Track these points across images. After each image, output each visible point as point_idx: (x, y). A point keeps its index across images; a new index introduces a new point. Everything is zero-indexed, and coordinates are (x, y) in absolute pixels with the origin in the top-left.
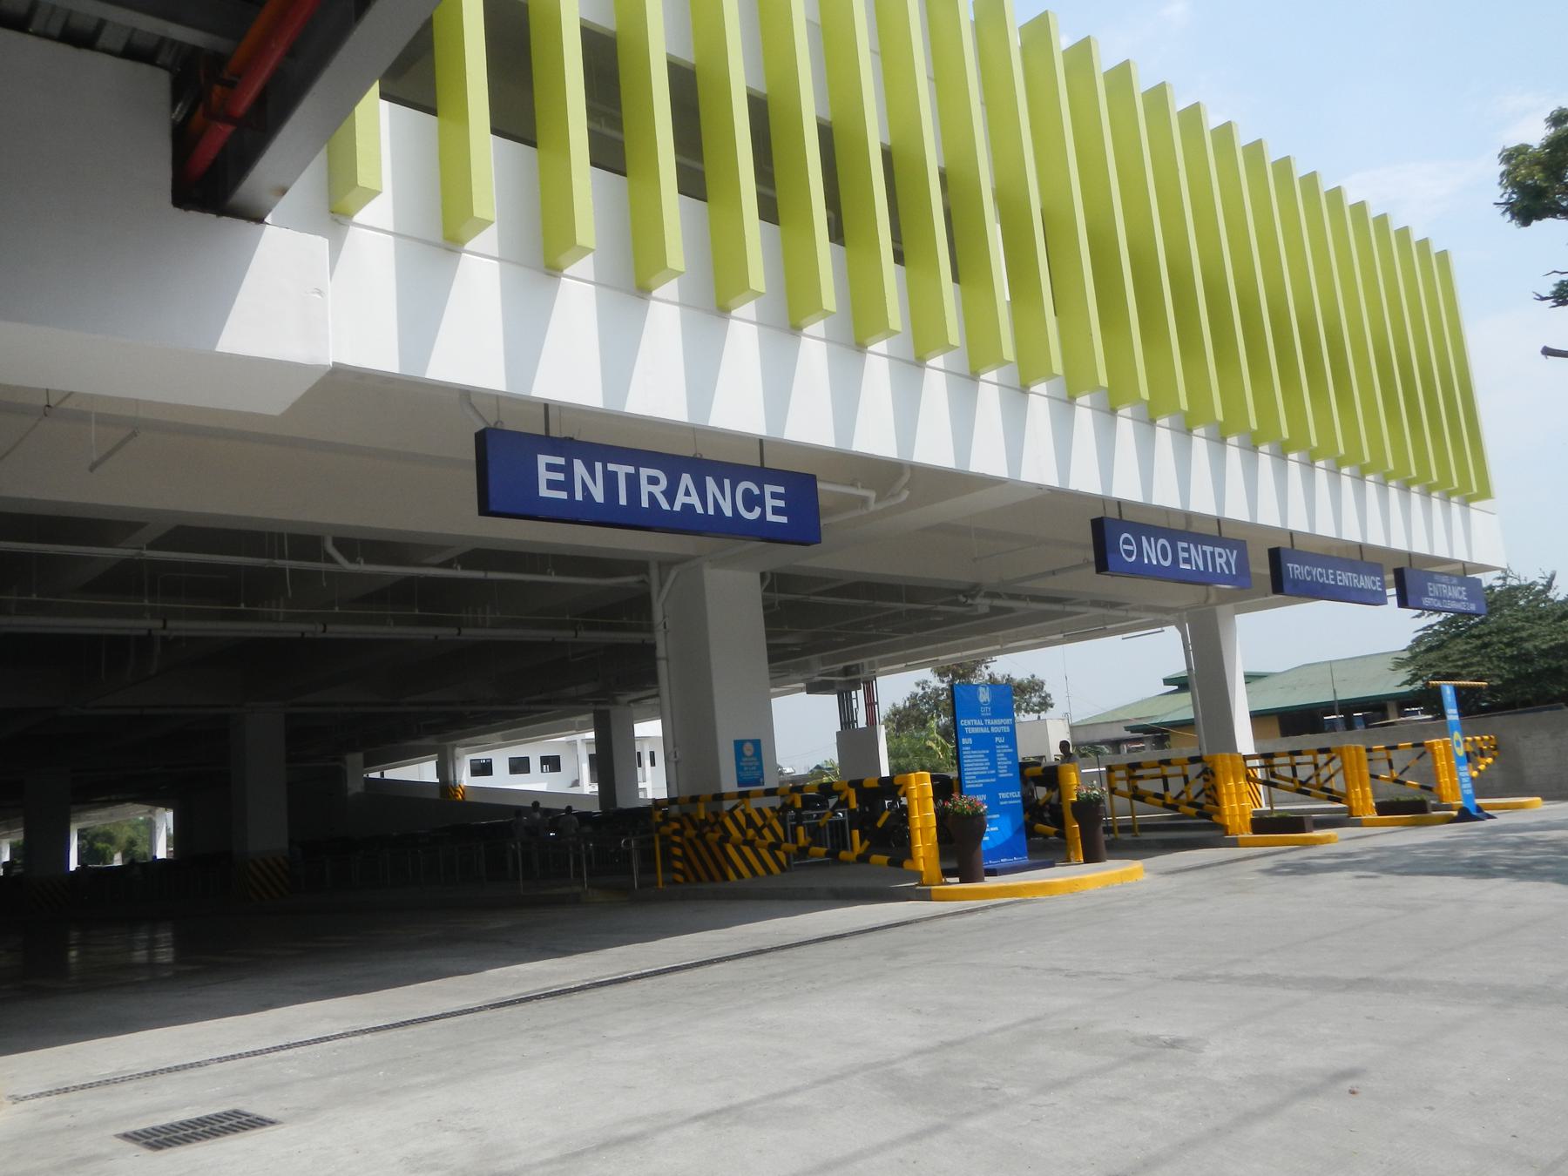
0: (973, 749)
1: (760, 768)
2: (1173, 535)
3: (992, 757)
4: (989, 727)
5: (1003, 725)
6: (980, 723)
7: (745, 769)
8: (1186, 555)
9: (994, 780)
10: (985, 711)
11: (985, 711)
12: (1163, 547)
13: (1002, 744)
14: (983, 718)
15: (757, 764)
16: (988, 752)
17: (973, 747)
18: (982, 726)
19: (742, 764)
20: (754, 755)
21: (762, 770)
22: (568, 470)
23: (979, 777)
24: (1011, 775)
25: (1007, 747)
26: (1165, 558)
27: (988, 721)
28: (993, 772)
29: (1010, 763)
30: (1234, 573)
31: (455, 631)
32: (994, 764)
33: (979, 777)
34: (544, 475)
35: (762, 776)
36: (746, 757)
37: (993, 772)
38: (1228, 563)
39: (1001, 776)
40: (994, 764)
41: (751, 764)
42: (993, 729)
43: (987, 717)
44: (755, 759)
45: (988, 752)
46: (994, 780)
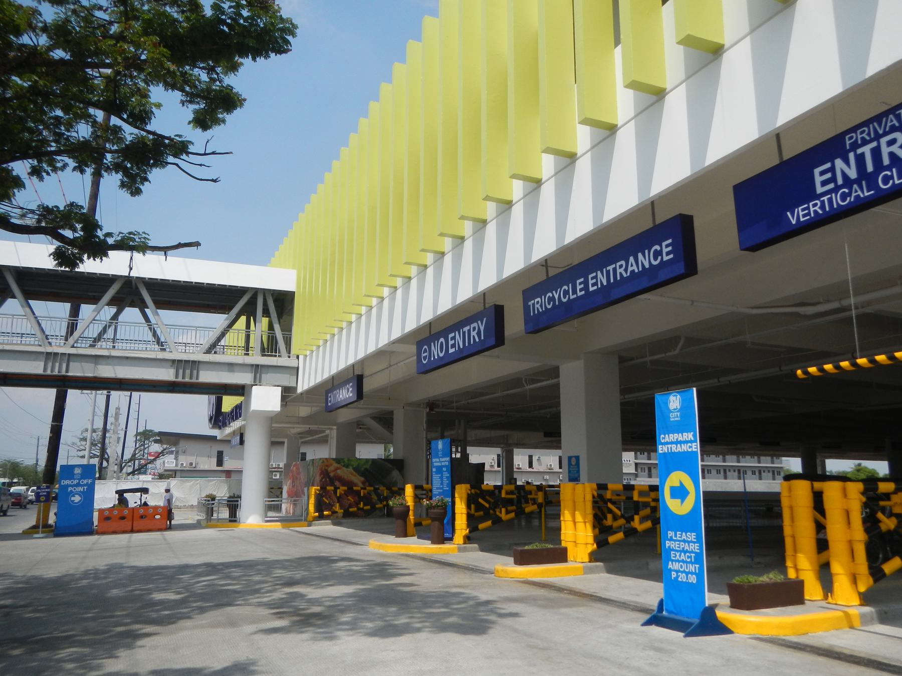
0: (436, 474)
1: (578, 472)
2: (444, 333)
3: (441, 478)
4: (441, 462)
5: (446, 461)
6: (438, 460)
7: (572, 472)
8: (453, 342)
9: (441, 491)
10: (440, 453)
11: (440, 453)
12: (442, 343)
13: (445, 471)
14: (439, 458)
15: (577, 469)
16: (440, 475)
17: (437, 473)
18: (438, 462)
19: (571, 469)
20: (575, 465)
21: (579, 473)
22: (330, 397)
23: (437, 488)
24: (448, 489)
25: (447, 473)
26: (441, 352)
27: (442, 460)
28: (442, 486)
29: (447, 482)
30: (482, 338)
31: (716, 380)
32: (442, 484)
33: (437, 488)
34: (329, 399)
35: (579, 476)
36: (573, 465)
37: (442, 486)
38: (479, 334)
39: (445, 489)
40: (442, 484)
41: (574, 469)
42: (443, 464)
43: (440, 457)
44: (576, 467)
45: (440, 475)
46: (441, 491)
